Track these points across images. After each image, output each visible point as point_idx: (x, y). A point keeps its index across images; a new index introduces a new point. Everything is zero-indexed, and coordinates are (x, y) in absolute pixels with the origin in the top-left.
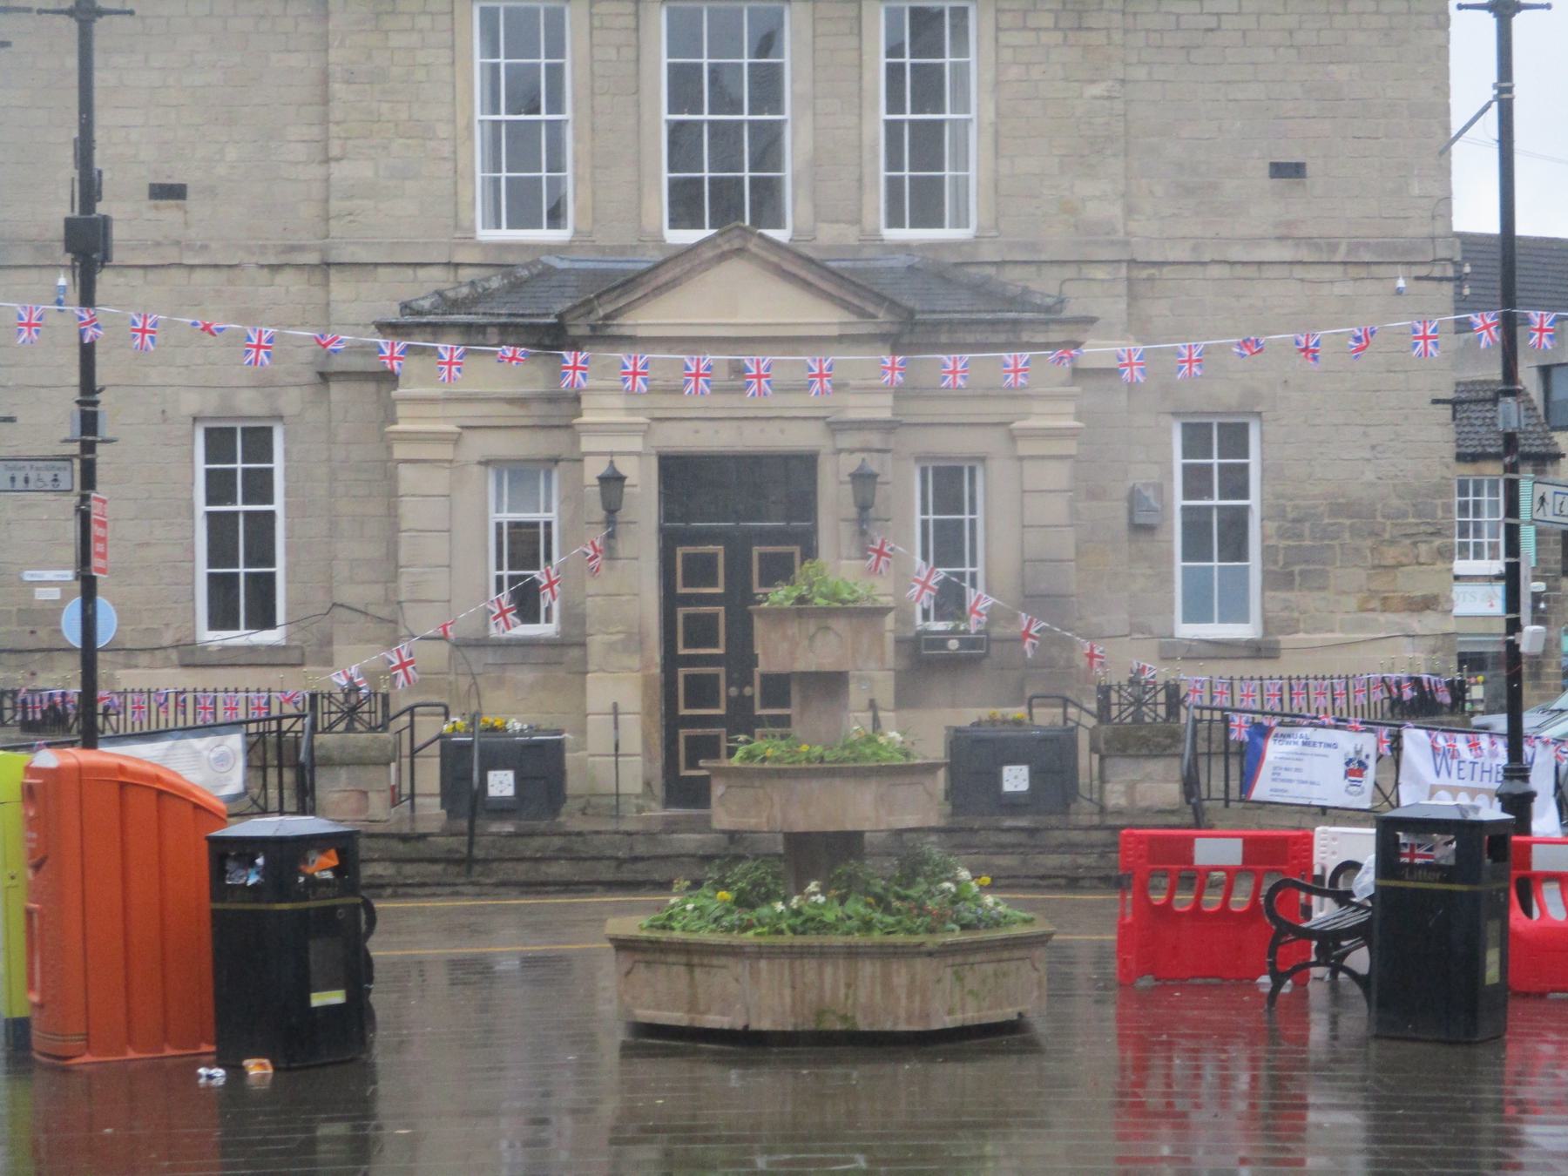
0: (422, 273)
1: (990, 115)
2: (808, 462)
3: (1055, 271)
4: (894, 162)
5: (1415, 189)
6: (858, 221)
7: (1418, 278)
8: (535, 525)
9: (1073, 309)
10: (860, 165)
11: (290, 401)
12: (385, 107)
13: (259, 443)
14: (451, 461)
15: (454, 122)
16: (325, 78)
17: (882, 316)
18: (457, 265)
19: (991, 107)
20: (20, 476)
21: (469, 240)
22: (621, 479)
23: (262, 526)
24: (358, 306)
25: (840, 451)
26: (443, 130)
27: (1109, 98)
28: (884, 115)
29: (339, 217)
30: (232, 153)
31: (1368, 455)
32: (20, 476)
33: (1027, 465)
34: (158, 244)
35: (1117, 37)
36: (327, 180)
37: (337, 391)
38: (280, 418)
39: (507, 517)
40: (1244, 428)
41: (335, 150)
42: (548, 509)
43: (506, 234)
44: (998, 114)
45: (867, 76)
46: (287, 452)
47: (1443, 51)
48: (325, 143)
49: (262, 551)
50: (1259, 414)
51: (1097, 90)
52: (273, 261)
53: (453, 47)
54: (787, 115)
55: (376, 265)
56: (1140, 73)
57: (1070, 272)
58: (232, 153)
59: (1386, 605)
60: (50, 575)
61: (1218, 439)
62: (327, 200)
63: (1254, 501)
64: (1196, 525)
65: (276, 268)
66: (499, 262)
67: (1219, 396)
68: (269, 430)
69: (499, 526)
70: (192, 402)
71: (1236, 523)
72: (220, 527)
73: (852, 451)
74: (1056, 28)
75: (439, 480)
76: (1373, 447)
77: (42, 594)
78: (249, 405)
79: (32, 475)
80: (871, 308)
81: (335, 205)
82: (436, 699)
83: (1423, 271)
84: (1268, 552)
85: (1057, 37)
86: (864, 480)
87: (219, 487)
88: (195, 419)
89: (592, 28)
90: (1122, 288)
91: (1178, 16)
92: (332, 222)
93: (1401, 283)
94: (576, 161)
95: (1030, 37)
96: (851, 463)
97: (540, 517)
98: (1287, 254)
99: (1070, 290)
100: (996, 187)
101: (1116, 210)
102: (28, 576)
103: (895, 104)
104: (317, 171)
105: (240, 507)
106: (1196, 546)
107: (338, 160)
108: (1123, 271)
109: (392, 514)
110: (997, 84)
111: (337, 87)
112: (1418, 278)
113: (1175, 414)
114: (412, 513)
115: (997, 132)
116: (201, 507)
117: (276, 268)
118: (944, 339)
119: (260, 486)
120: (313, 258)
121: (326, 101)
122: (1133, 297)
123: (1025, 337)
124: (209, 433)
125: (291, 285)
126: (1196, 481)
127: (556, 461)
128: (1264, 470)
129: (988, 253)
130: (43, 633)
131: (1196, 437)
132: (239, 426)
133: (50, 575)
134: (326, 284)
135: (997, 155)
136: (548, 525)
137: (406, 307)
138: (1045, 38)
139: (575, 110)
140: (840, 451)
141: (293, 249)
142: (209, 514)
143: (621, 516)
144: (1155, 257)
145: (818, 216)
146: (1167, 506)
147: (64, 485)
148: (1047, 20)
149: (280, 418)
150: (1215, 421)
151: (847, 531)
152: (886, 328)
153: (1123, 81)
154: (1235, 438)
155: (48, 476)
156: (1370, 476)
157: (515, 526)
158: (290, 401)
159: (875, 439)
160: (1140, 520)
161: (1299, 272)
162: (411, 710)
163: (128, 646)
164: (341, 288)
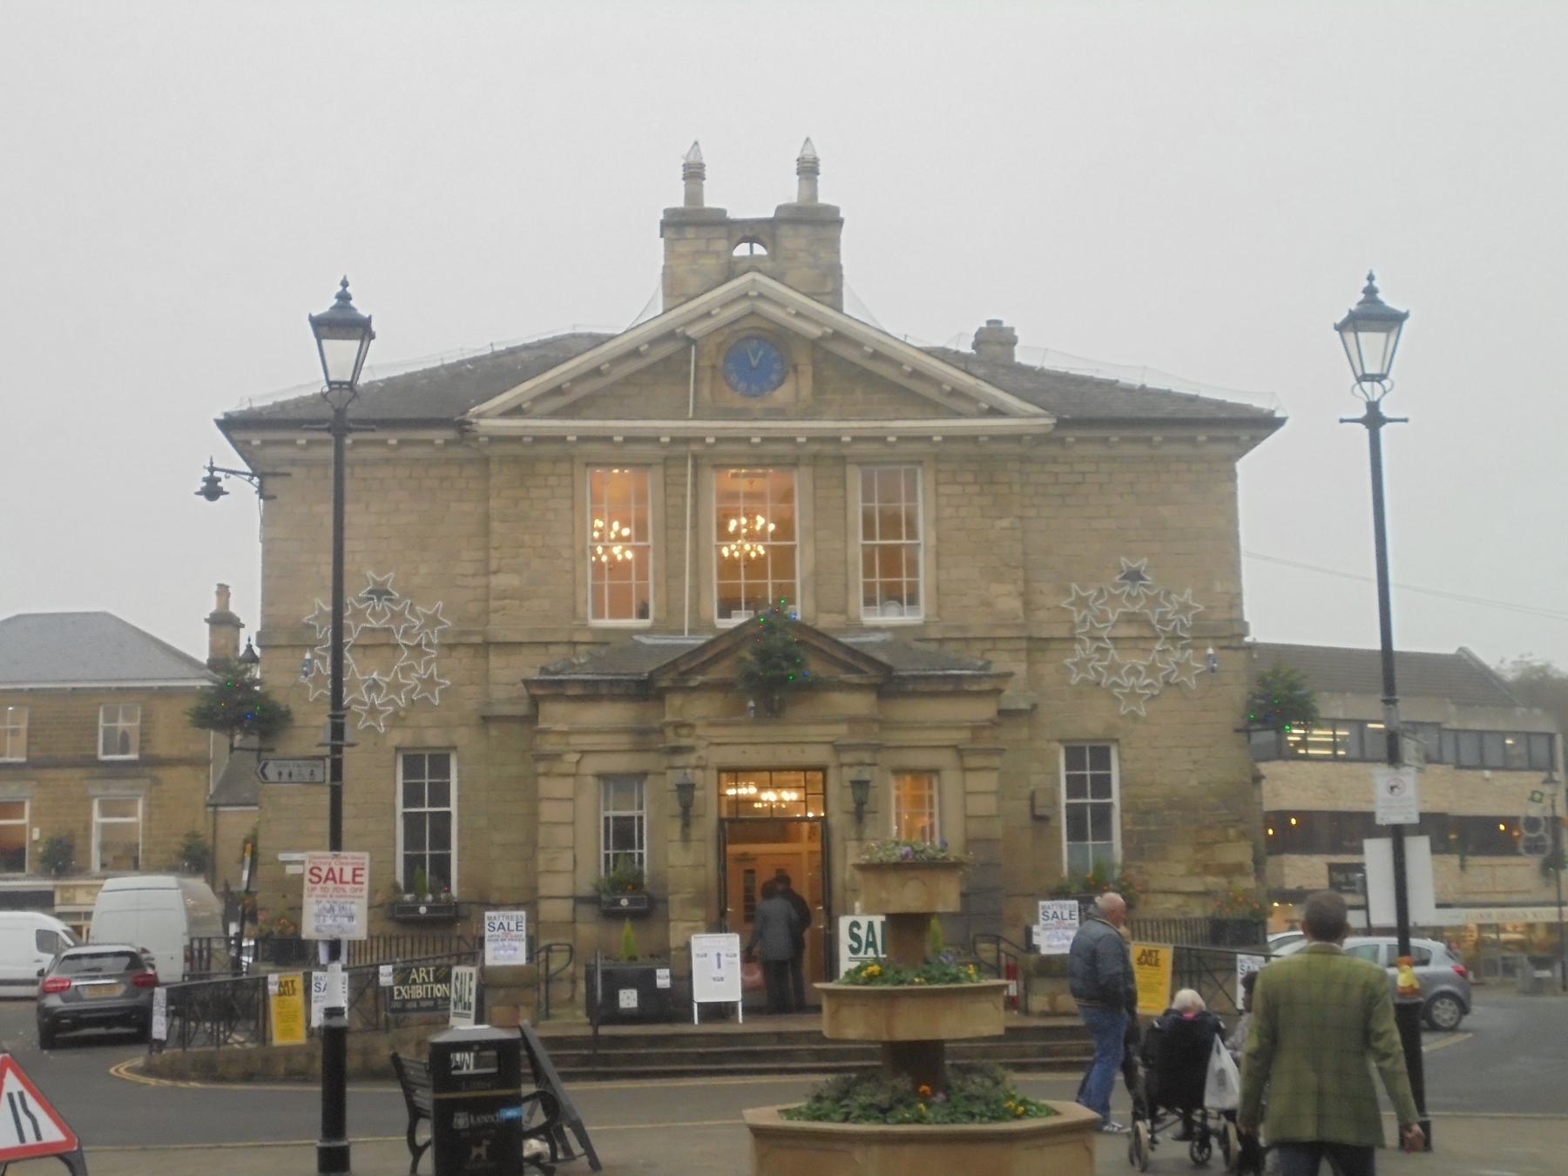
0: (553, 649)
1: (932, 541)
2: (823, 769)
3: (979, 645)
4: (869, 571)
5: (1218, 587)
6: (844, 611)
7: (1222, 648)
8: (631, 818)
9: (994, 670)
10: (846, 574)
11: (462, 736)
12: (526, 538)
13: (440, 763)
14: (573, 775)
15: (572, 547)
16: (487, 518)
17: (872, 673)
18: (575, 643)
19: (933, 534)
20: (285, 772)
21: (585, 628)
22: (692, 786)
24: (508, 676)
25: (842, 765)
26: (566, 553)
27: (1013, 529)
28: (860, 540)
29: (496, 611)
30: (423, 569)
31: (1191, 767)
32: (285, 772)
33: (969, 775)
35: (1017, 488)
36: (487, 586)
37: (494, 732)
38: (455, 748)
39: (612, 813)
40: (1107, 750)
41: (494, 565)
42: (641, 808)
43: (607, 622)
44: (938, 539)
45: (850, 516)
46: (459, 772)
47: (1232, 496)
48: (487, 561)
49: (441, 838)
50: (1116, 741)
51: (1005, 523)
52: (451, 641)
53: (572, 498)
54: (797, 542)
55: (521, 644)
56: (1032, 512)
57: (988, 645)
58: (423, 569)
59: (1207, 869)
60: (296, 856)
61: (1089, 759)
62: (487, 600)
63: (1115, 798)
64: (1075, 815)
66: (604, 639)
67: (1091, 723)
68: (447, 757)
69: (607, 819)
70: (397, 737)
71: (1102, 815)
72: (413, 823)
73: (850, 765)
74: (975, 483)
75: (562, 788)
76: (1195, 762)
77: (291, 870)
78: (434, 738)
79: (295, 771)
80: (866, 669)
81: (494, 604)
82: (562, 940)
83: (1224, 643)
84: (1126, 836)
85: (977, 488)
86: (860, 786)
87: (413, 795)
88: (397, 749)
89: (666, 485)
90: (1023, 656)
91: (1056, 474)
92: (492, 616)
93: (1210, 651)
94: (655, 573)
95: (957, 489)
96: (851, 774)
97: (635, 813)
98: (1132, 631)
99: (989, 656)
100: (938, 589)
101: (1016, 604)
102: (282, 857)
103: (869, 534)
104: (481, 581)
105: (426, 809)
106: (1077, 833)
107: (495, 573)
108: (1024, 644)
109: (535, 814)
110: (938, 519)
111: (496, 525)
112: (1222, 648)
113: (1060, 741)
114: (548, 811)
115: (938, 554)
116: (400, 809)
117: (451, 647)
118: (910, 687)
119: (440, 795)
120: (477, 639)
121: (487, 533)
122: (1031, 663)
123: (966, 687)
124: (406, 758)
126: (1075, 787)
127: (643, 775)
128: (1122, 779)
129: (934, 633)
131: (1075, 757)
134: (487, 657)
135: (938, 567)
136: (640, 818)
137: (544, 670)
138: (971, 489)
139: (655, 538)
140: (842, 765)
141: (464, 633)
142: (405, 814)
143: (692, 811)
144: (1045, 634)
145: (819, 609)
146: (1055, 803)
147: (319, 778)
148: (969, 478)
149: (455, 748)
150: (1087, 746)
152: (874, 680)
153: (1021, 518)
154: (1101, 757)
155: (306, 772)
156: (1193, 782)
157: (616, 819)
158: (462, 736)
159: (866, 757)
160: (1038, 812)
161: (1142, 644)
162: (548, 949)
164: (496, 661)
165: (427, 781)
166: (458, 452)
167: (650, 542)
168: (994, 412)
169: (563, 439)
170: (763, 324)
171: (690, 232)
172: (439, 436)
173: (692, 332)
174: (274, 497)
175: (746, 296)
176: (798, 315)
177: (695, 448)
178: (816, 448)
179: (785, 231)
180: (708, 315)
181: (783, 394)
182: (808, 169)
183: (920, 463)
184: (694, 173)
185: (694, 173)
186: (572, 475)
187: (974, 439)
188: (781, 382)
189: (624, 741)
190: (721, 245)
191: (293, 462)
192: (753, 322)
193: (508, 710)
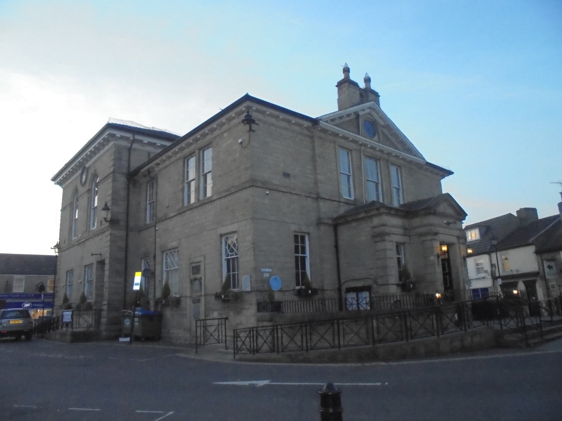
11: (311, 229)
18: (340, 202)
23: (303, 259)
34: (286, 187)
37: (323, 228)
38: (309, 234)
52: (308, 195)
60: (267, 270)
65: (306, 197)
70: (294, 228)
78: (304, 229)
81: (319, 185)
88: (295, 232)
102: (263, 270)
105: (300, 255)
120: (314, 196)
125: (310, 203)
130: (266, 287)
132: (299, 234)
133: (267, 270)
141: (310, 193)
149: (309, 234)
151: (462, 260)
158: (311, 229)
163: (283, 289)
164: (321, 204)
165: (300, 245)
166: (306, 132)
167: (351, 174)
168: (415, 156)
169: (336, 135)
170: (370, 117)
171: (352, 86)
172: (306, 124)
173: (361, 113)
174: (254, 131)
175: (370, 108)
176: (381, 118)
177: (363, 148)
178: (385, 155)
179: (370, 94)
180: (364, 110)
181: (376, 138)
182: (367, 80)
183: (400, 167)
184: (346, 70)
185: (346, 70)
186: (335, 148)
187: (410, 162)
188: (374, 135)
189: (401, 231)
190: (358, 93)
191: (259, 120)
192: (369, 116)
193: (326, 221)
